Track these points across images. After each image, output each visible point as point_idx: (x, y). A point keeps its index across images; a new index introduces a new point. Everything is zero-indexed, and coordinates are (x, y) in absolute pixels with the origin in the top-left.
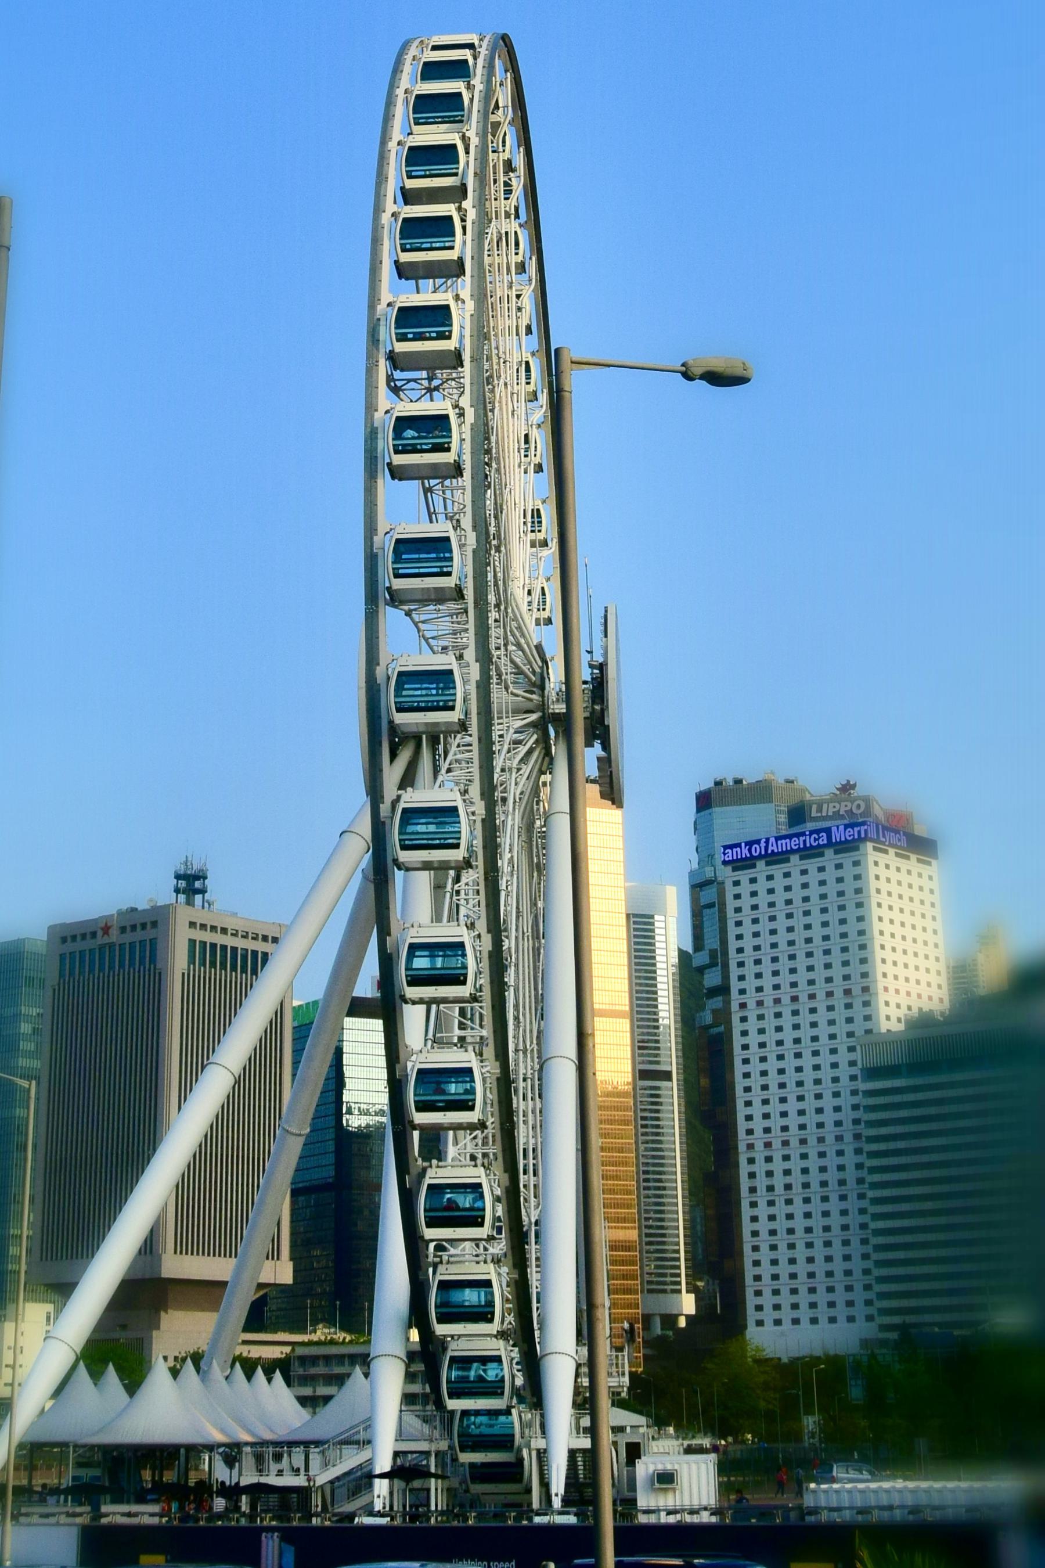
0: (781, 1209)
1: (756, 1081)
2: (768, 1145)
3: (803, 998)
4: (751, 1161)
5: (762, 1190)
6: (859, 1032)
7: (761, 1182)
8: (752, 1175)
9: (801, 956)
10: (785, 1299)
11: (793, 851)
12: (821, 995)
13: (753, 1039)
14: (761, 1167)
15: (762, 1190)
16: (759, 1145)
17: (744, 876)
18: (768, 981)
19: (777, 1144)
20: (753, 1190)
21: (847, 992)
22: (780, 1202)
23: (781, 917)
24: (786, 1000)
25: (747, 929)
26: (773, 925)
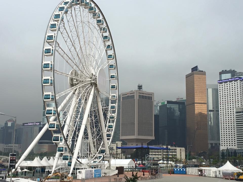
0: (225, 131)
1: (222, 113)
2: (224, 122)
3: (229, 102)
4: (221, 124)
5: (223, 128)
6: (237, 107)
7: (223, 127)
8: (221, 126)
9: (229, 96)
10: (226, 143)
11: (228, 81)
12: (232, 101)
13: (222, 107)
14: (223, 125)
15: (223, 128)
16: (222, 122)
17: (221, 85)
18: (224, 99)
19: (225, 122)
20: (221, 128)
21: (235, 101)
22: (225, 130)
23: (226, 90)
24: (227, 102)
25: (221, 92)
26: (225, 92)
